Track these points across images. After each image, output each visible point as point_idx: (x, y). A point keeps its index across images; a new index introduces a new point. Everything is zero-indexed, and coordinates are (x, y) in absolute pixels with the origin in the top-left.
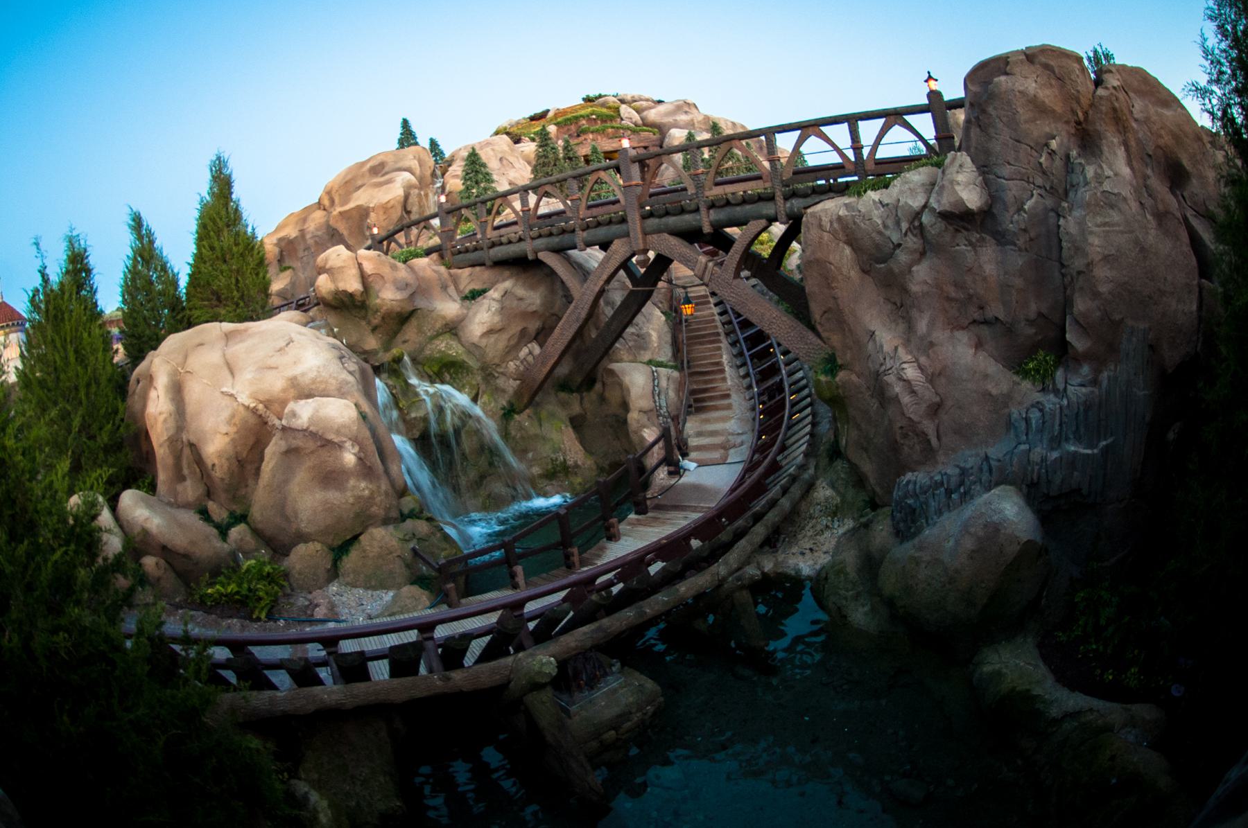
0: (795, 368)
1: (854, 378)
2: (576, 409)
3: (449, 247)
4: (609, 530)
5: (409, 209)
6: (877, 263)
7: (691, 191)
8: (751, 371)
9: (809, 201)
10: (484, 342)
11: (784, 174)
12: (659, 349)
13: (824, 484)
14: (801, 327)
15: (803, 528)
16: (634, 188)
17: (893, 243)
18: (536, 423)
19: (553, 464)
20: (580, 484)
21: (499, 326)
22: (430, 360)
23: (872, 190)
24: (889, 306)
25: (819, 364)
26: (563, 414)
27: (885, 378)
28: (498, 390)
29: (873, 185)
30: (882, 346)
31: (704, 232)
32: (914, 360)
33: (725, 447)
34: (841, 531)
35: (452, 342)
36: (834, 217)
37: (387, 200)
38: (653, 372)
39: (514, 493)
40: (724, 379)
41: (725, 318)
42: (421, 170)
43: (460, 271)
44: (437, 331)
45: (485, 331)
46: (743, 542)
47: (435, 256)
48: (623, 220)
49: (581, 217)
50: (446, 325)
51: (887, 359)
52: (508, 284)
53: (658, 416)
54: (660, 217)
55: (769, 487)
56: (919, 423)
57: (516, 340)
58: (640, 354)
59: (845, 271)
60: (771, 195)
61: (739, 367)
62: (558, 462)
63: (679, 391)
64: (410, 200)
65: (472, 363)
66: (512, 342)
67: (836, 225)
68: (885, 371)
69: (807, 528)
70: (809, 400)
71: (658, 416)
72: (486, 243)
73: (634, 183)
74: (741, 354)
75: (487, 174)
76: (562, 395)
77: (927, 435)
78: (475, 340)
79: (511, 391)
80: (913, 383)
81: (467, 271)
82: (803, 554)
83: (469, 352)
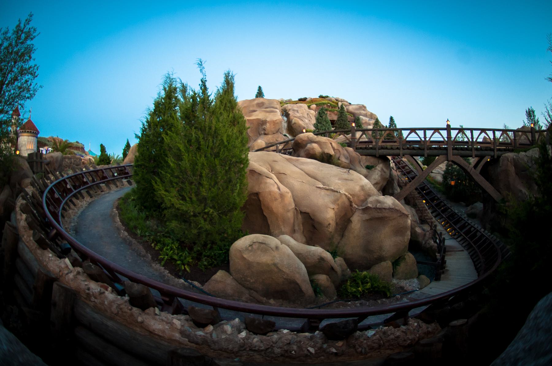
3: (355, 145)
37: (275, 120)
81: (364, 157)
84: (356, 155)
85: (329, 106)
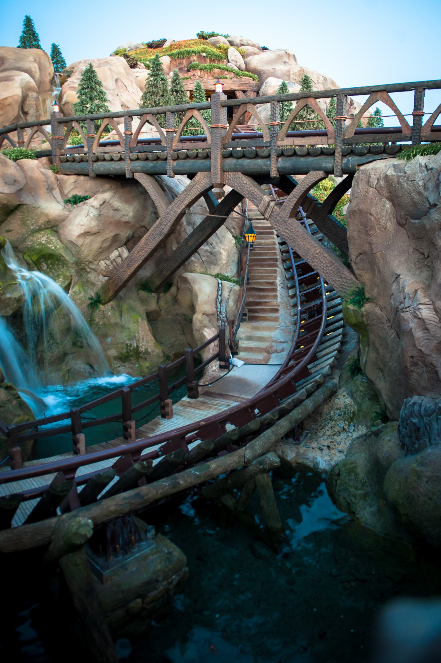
0: (334, 295)
1: (377, 310)
2: (153, 306)
3: (58, 154)
4: (165, 409)
5: (26, 110)
6: (412, 218)
7: (266, 139)
8: (298, 293)
9: (363, 159)
10: (80, 242)
11: (347, 134)
12: (227, 266)
13: (345, 393)
14: (339, 264)
15: (323, 428)
16: (220, 130)
17: (430, 203)
18: (117, 314)
19: (127, 349)
20: (148, 367)
21: (95, 230)
22: (31, 250)
23: (422, 155)
24: (418, 255)
25: (350, 295)
26: (141, 309)
27: (402, 314)
28: (88, 283)
29: (424, 151)
30: (404, 288)
31: (271, 176)
32: (431, 303)
33: (269, 351)
34: (355, 435)
35: (52, 238)
36: (382, 176)
38: (219, 284)
39: (91, 371)
40: (275, 297)
41: (283, 248)
42: (41, 75)
43: (66, 177)
44: (40, 226)
45: (82, 232)
46: (268, 432)
47: (44, 160)
48: (208, 157)
49: (174, 148)
50: (48, 222)
51: (407, 299)
52: (107, 195)
53: (218, 320)
54: (238, 158)
55: (298, 388)
56: (429, 356)
57: (108, 244)
58: (210, 268)
59: (382, 222)
60: (332, 152)
61: (289, 288)
62: (132, 348)
63: (238, 301)
64: (28, 102)
65: (68, 257)
66: (105, 245)
67: (382, 183)
68: (403, 308)
69: (327, 428)
70: (342, 322)
71: (218, 320)
72: (90, 157)
73: (220, 125)
74: (292, 278)
75: (101, 92)
76: (143, 293)
77: (435, 367)
78: (73, 238)
79: (99, 285)
80: (426, 321)
81: (72, 178)
82: (321, 449)
83: (66, 248)
84: (41, 176)
85: (204, 57)
